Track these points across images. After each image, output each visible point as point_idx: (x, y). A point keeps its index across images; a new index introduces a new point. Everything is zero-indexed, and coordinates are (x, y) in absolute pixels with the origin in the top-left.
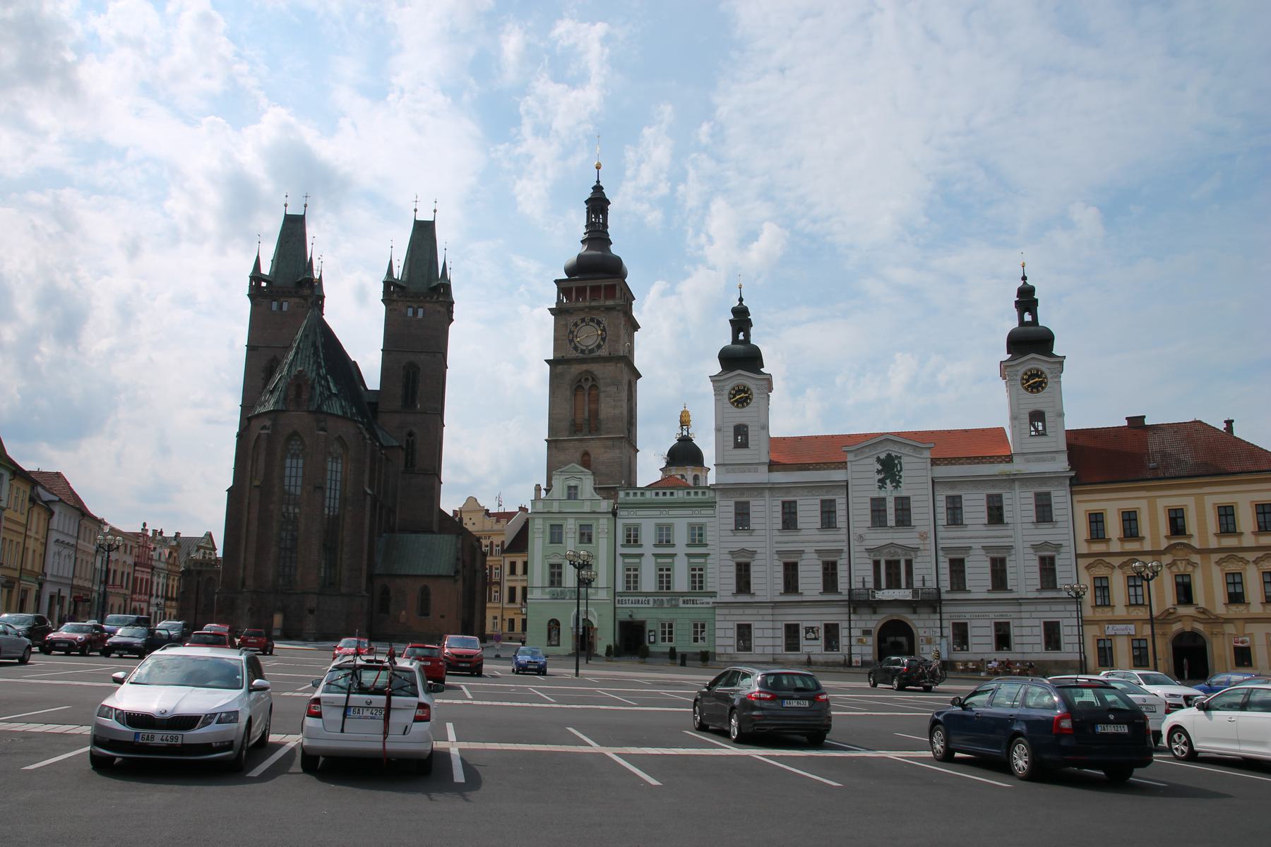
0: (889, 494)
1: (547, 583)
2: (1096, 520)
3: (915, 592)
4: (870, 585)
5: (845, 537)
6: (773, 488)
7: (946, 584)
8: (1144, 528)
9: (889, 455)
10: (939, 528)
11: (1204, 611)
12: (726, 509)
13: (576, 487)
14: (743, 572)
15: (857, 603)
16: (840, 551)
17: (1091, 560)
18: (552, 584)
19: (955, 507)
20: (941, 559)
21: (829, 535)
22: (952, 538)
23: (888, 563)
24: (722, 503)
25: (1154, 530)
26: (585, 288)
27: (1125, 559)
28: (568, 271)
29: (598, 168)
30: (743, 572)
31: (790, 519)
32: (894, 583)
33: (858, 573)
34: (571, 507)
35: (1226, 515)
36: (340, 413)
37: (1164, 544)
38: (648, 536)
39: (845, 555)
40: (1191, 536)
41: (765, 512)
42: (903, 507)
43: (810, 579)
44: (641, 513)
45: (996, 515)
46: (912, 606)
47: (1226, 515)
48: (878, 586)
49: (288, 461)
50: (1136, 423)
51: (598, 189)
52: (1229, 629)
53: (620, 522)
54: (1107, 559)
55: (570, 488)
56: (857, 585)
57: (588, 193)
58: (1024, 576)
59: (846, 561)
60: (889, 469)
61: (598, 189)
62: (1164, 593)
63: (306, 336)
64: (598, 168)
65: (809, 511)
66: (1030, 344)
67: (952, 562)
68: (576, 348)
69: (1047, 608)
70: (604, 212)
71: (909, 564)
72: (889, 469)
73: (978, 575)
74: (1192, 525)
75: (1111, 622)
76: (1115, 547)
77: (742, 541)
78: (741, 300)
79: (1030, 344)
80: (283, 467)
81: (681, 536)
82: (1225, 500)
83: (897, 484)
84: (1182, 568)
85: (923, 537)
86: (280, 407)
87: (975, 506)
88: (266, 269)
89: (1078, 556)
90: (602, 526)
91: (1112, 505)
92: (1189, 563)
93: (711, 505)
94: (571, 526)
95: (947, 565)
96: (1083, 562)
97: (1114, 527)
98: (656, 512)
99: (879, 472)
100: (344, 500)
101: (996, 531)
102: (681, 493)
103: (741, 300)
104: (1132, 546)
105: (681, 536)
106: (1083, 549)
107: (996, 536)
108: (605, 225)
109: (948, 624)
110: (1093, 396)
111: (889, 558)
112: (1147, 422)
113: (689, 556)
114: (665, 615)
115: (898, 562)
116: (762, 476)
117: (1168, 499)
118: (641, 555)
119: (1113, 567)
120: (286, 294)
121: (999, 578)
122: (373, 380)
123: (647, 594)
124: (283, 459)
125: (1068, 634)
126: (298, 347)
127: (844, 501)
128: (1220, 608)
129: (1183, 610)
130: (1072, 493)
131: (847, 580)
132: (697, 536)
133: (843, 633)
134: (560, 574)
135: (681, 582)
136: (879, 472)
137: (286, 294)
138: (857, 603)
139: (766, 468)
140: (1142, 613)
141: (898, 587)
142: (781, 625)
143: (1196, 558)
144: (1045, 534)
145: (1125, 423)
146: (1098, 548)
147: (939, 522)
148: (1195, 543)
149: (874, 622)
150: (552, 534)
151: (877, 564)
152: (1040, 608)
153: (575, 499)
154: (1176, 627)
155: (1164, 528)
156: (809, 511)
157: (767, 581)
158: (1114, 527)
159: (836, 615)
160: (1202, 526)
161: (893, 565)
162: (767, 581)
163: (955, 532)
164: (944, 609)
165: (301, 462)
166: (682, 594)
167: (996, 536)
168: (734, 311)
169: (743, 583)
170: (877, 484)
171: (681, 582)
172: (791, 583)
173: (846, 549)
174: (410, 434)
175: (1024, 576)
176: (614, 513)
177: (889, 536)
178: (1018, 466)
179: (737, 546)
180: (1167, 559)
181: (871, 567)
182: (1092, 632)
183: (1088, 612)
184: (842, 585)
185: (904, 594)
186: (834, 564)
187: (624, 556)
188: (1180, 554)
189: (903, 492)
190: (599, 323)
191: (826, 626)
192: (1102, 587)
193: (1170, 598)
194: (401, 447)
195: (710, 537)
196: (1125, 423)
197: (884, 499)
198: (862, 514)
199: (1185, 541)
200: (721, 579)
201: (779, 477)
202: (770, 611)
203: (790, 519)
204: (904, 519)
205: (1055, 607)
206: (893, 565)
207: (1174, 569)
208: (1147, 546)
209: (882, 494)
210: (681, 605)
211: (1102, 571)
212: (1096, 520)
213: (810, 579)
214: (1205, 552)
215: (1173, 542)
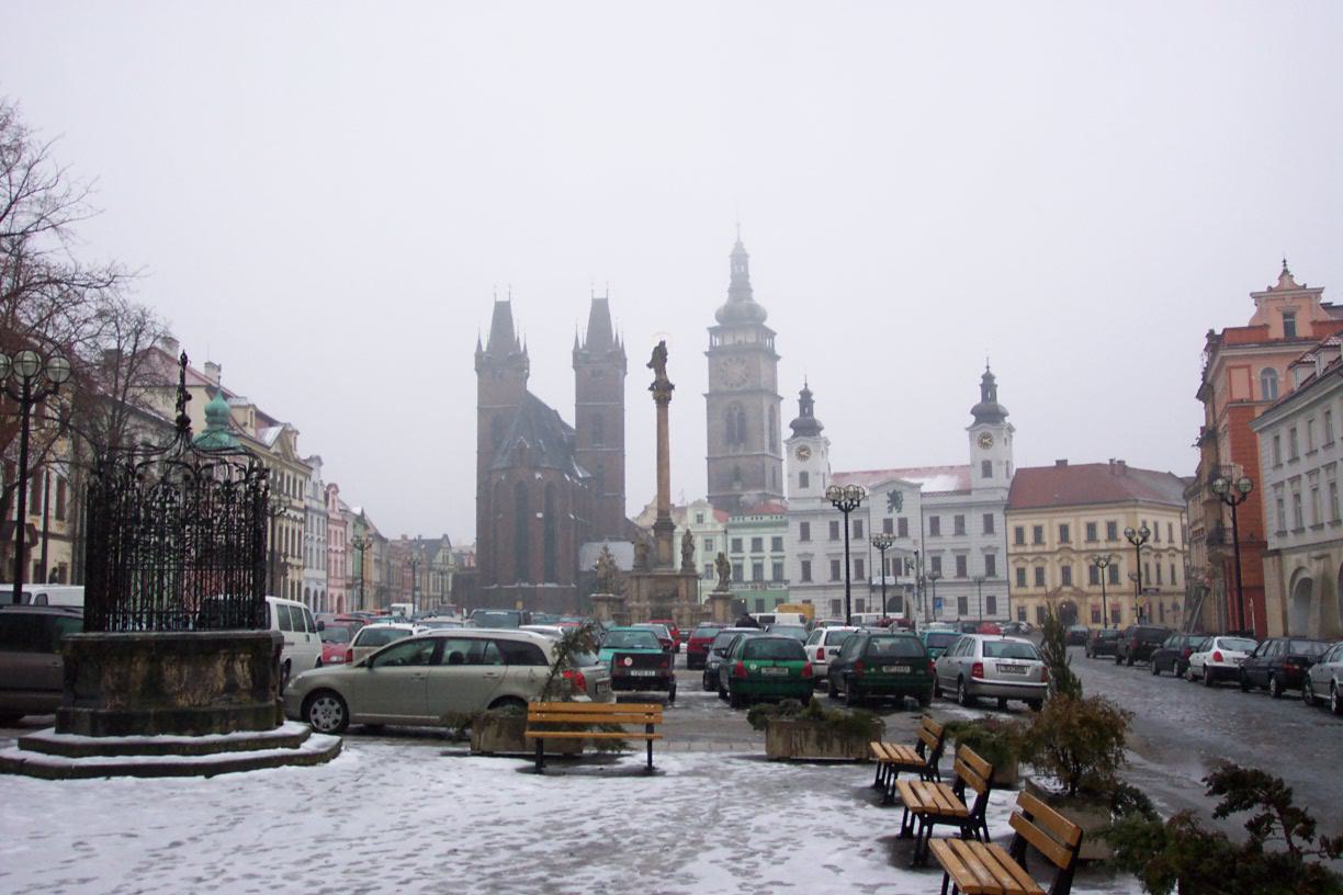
0: (895, 516)
2: (1019, 532)
10: (925, 539)
11: (1076, 589)
13: (702, 516)
14: (806, 567)
19: (935, 522)
22: (933, 544)
23: (894, 560)
25: (1051, 538)
28: (718, 317)
29: (738, 225)
30: (806, 567)
35: (1091, 528)
37: (1057, 547)
38: (747, 545)
39: (868, 556)
40: (1071, 542)
42: (903, 523)
47: (1091, 528)
50: (1062, 464)
51: (739, 245)
52: (1090, 600)
53: (730, 538)
54: (1025, 557)
57: (729, 249)
60: (895, 500)
61: (739, 245)
62: (1053, 578)
64: (738, 225)
66: (988, 414)
67: (933, 559)
68: (726, 384)
70: (746, 265)
72: (895, 500)
73: (949, 569)
75: (1027, 596)
76: (1030, 549)
79: (988, 414)
81: (767, 545)
82: (1091, 519)
83: (900, 510)
84: (1064, 563)
85: (915, 542)
87: (947, 523)
88: (484, 349)
89: (1008, 555)
91: (1028, 523)
92: (1069, 558)
93: (785, 524)
95: (930, 561)
96: (1011, 559)
97: (1029, 537)
98: (751, 530)
101: (960, 539)
104: (1039, 548)
105: (767, 545)
106: (1011, 550)
107: (960, 543)
108: (747, 276)
110: (1031, 448)
112: (1069, 463)
113: (772, 557)
114: (760, 595)
116: (817, 505)
118: (742, 558)
119: (1027, 561)
120: (501, 363)
122: (569, 417)
123: (748, 582)
125: (1001, 604)
128: (1086, 588)
129: (1065, 589)
130: (1006, 515)
132: (777, 544)
133: (984, 608)
135: (768, 574)
137: (501, 363)
139: (819, 500)
140: (1041, 590)
143: (1073, 556)
144: (990, 540)
145: (1054, 464)
146: (1020, 549)
147: (925, 535)
148: (1074, 547)
154: (1061, 599)
155: (1057, 537)
158: (1029, 537)
160: (1078, 537)
163: (935, 540)
166: (769, 583)
168: (801, 393)
169: (807, 575)
171: (768, 574)
176: (726, 532)
178: (974, 497)
179: (801, 551)
180: (1058, 557)
182: (1015, 603)
183: (1013, 590)
184: (867, 575)
186: (862, 561)
189: (902, 515)
190: (743, 362)
192: (1021, 573)
193: (1059, 581)
196: (1054, 464)
199: (1068, 545)
200: (792, 572)
208: (1047, 548)
210: (769, 589)
211: (1021, 565)
212: (1019, 532)
214: (1079, 552)
215: (1062, 546)
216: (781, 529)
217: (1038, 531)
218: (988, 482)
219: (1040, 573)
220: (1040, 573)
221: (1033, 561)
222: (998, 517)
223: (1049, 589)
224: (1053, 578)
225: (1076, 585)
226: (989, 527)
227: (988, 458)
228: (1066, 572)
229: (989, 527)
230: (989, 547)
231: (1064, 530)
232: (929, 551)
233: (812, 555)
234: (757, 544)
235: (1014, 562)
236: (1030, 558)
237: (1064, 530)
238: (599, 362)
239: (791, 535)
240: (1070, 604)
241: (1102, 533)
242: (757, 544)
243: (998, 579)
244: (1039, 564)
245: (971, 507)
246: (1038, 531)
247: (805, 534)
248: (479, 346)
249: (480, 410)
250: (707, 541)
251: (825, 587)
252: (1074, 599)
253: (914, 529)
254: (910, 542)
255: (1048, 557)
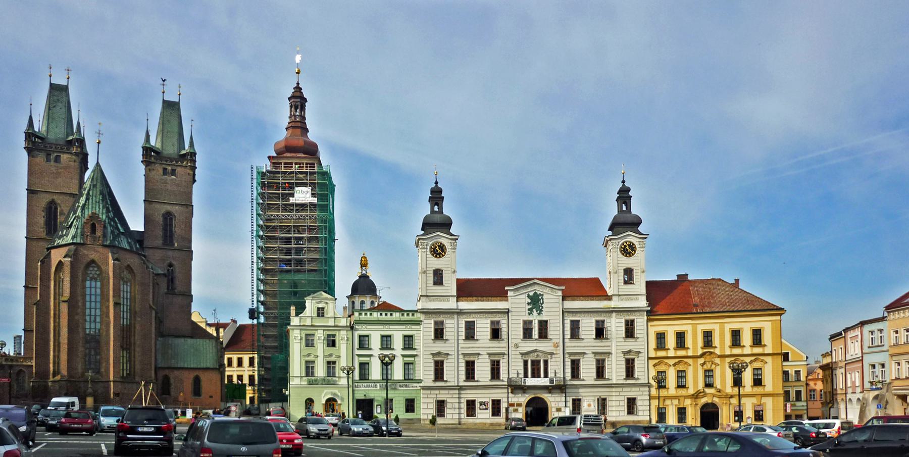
0: (535, 318)
1: (304, 374)
2: (661, 338)
3: (551, 381)
4: (522, 375)
5: (506, 345)
6: (460, 313)
7: (568, 375)
8: (689, 342)
9: (535, 293)
10: (566, 340)
12: (428, 325)
13: (323, 309)
15: (516, 388)
16: (504, 354)
17: (657, 361)
18: (307, 375)
19: (575, 326)
20: (567, 360)
21: (495, 344)
22: (573, 346)
23: (533, 362)
24: (426, 321)
25: (694, 344)
26: (291, 164)
27: (677, 360)
31: (470, 334)
32: (536, 374)
33: (513, 369)
34: (319, 322)
35: (736, 335)
36: (128, 248)
37: (700, 352)
41: (454, 328)
42: (543, 325)
43: (483, 371)
44: (369, 327)
45: (600, 333)
46: (549, 389)
47: (736, 335)
48: (526, 376)
49: (88, 283)
53: (356, 334)
54: (666, 361)
55: (319, 309)
56: (513, 375)
57: (290, 92)
58: (615, 370)
59: (506, 360)
60: (536, 302)
61: (298, 89)
63: (95, 186)
65: (483, 328)
69: (629, 389)
70: (303, 108)
71: (546, 362)
74: (716, 341)
76: (671, 353)
77: (439, 347)
78: (436, 183)
80: (84, 287)
86: (78, 240)
89: (649, 358)
90: (342, 336)
91: (670, 328)
93: (418, 323)
94: (320, 335)
96: (652, 362)
97: (671, 341)
98: (381, 327)
99: (529, 304)
100: (133, 313)
102: (398, 314)
103: (436, 183)
104: (681, 353)
106: (652, 354)
108: (304, 118)
109: (570, 400)
111: (534, 359)
113: (403, 356)
115: (539, 361)
116: (452, 304)
117: (705, 325)
118: (370, 356)
121: (600, 372)
123: (375, 382)
124: (84, 281)
126: (88, 194)
127: (506, 322)
131: (506, 372)
132: (408, 342)
134: (313, 368)
135: (398, 372)
136: (529, 304)
138: (516, 388)
141: (539, 376)
142: (464, 401)
143: (717, 360)
144: (630, 345)
146: (661, 354)
148: (717, 351)
149: (523, 399)
150: (307, 340)
151: (526, 363)
152: (625, 389)
153: (323, 316)
155: (700, 343)
156: (483, 328)
157: (454, 372)
158: (671, 341)
159: (501, 395)
161: (536, 363)
162: (454, 372)
164: (567, 390)
165: (99, 284)
166: (399, 381)
167: (600, 346)
169: (439, 374)
170: (527, 312)
171: (398, 372)
172: (470, 373)
173: (506, 352)
174: (170, 265)
175: (615, 370)
176: (352, 328)
177: (534, 344)
178: (614, 303)
179: (435, 350)
180: (701, 361)
181: (522, 364)
184: (503, 375)
185: (542, 381)
186: (498, 362)
187: (359, 356)
188: (708, 358)
189: (544, 317)
191: (493, 401)
194: (164, 275)
195: (419, 343)
197: (531, 322)
198: (517, 331)
199: (712, 350)
200: (424, 371)
201: (465, 305)
202: (457, 392)
203: (470, 334)
204: (543, 334)
205: (633, 389)
206: (536, 363)
207: (705, 367)
208: (690, 353)
209: (530, 318)
211: (662, 368)
212: (661, 338)
213: (483, 371)
214: (722, 357)
216: (414, 327)
217: (681, 336)
218: (628, 289)
219: (681, 375)
220: (681, 375)
221: (674, 365)
222: (640, 322)
223: (691, 391)
224: (695, 380)
225: (719, 387)
226: (630, 332)
227: (630, 266)
228: (709, 374)
229: (630, 332)
230: (630, 352)
231: (708, 335)
232: (570, 354)
233: (448, 354)
234: (386, 341)
235: (655, 366)
236: (672, 362)
237: (708, 335)
238: (169, 163)
239: (424, 333)
240: (714, 405)
241: (747, 339)
242: (386, 341)
243: (640, 382)
244: (681, 367)
245: (612, 312)
246: (681, 336)
247: (439, 334)
248: (31, 123)
249: (31, 192)
250: (328, 336)
251: (461, 388)
252: (716, 400)
253: (554, 331)
254: (551, 344)
255: (690, 361)
